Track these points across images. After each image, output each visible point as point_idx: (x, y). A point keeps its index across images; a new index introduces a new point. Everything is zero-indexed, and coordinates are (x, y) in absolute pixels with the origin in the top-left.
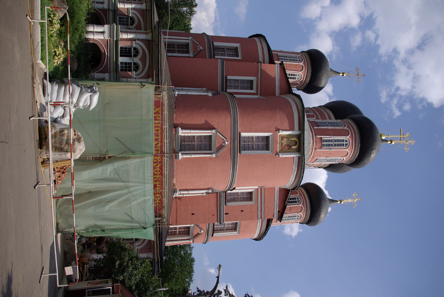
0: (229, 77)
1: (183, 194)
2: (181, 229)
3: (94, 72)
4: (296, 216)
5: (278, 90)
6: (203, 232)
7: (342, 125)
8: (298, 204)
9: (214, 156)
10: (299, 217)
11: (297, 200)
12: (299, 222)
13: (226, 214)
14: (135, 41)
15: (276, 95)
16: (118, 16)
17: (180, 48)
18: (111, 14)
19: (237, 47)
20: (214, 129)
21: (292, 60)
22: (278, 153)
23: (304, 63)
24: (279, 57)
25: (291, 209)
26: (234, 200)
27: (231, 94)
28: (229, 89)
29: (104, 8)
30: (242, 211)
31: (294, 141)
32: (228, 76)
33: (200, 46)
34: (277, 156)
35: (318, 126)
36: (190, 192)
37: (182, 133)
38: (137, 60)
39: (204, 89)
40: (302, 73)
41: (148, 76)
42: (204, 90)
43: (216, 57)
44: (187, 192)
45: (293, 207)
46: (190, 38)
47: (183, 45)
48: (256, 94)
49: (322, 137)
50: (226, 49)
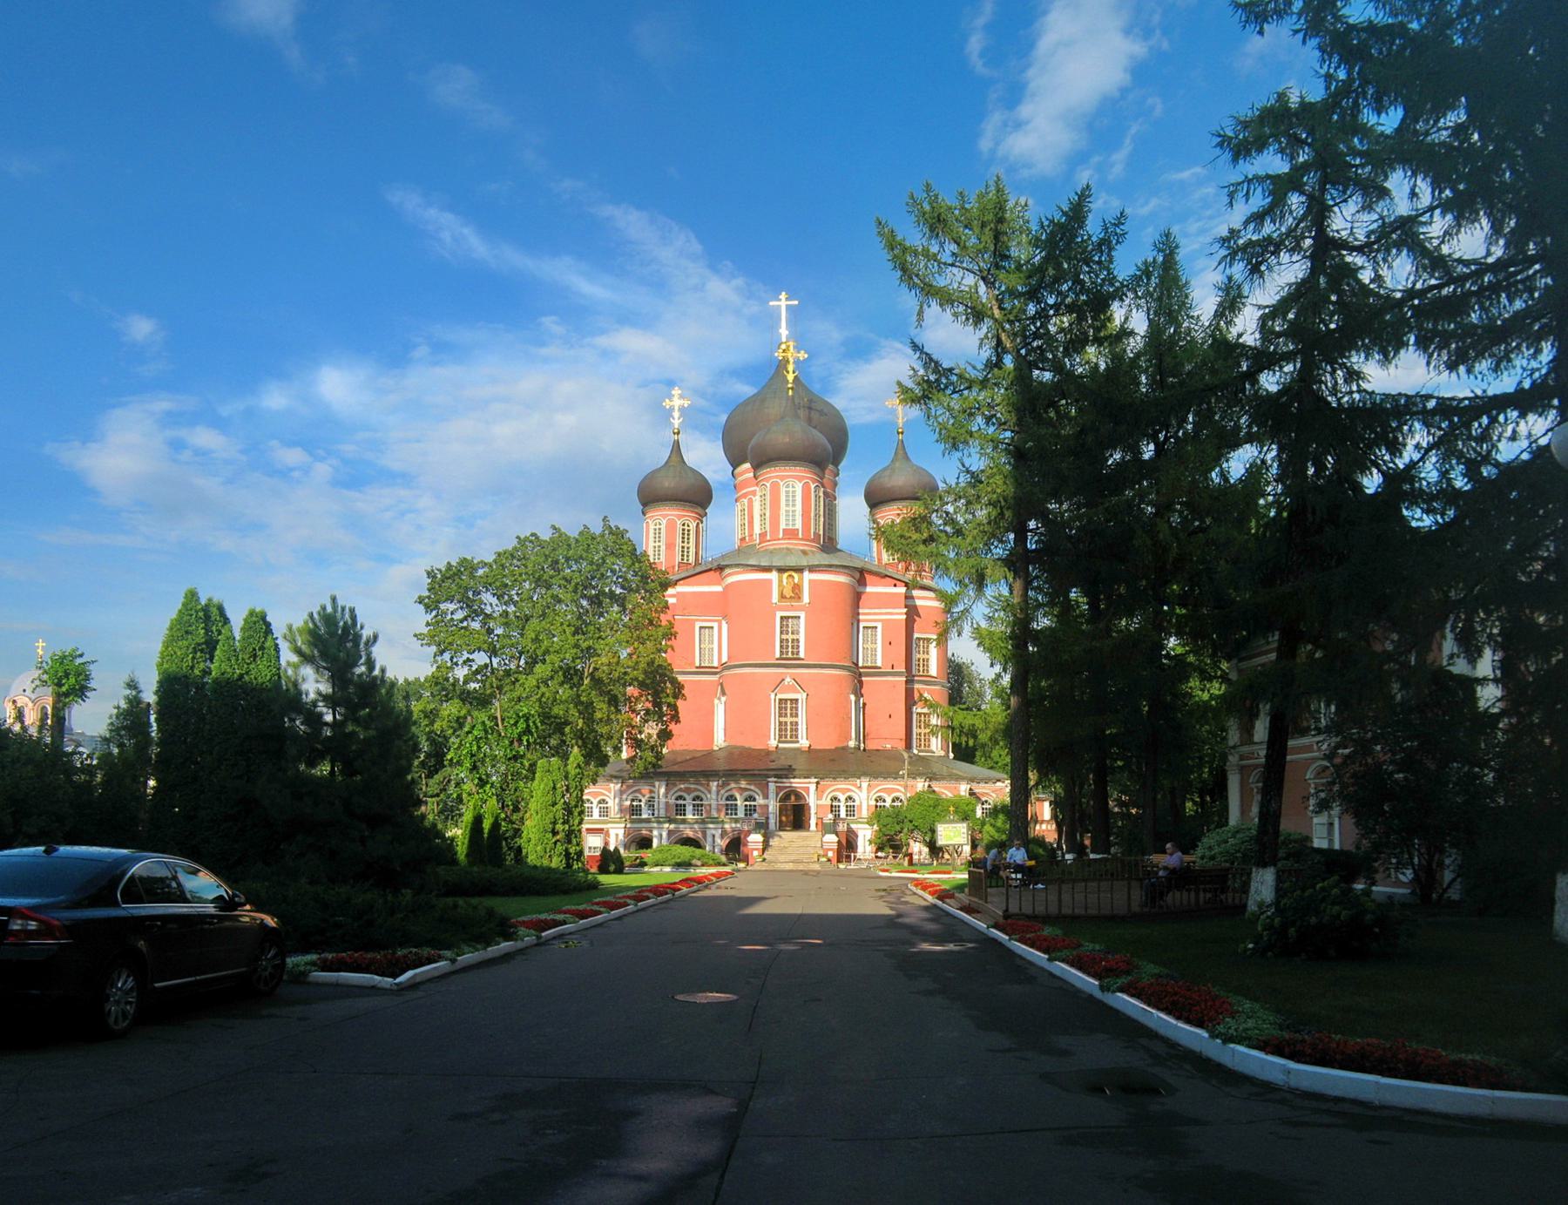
23: (664, 516)
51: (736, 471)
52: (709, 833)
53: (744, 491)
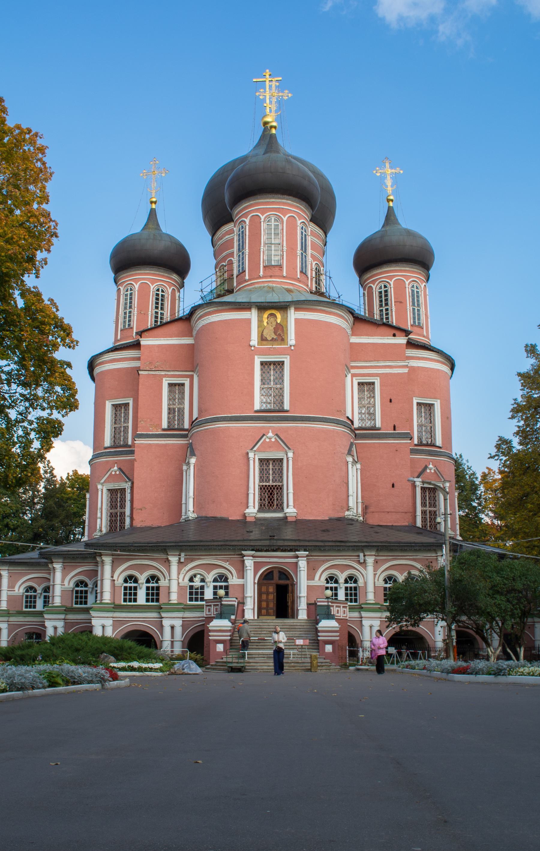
0: (165, 425)
1: (357, 502)
2: (425, 503)
3: (162, 641)
4: (413, 291)
5: (184, 339)
6: (432, 464)
7: (242, 227)
8: (391, 288)
9: (290, 455)
10: (415, 285)
11: (383, 290)
12: (424, 284)
13: (394, 429)
14: (114, 580)
15: (193, 342)
16: (75, 606)
17: (117, 504)
18: (70, 616)
19: (113, 405)
20: (248, 454)
21: (131, 303)
22: (289, 346)
24: (127, 327)
25: (399, 300)
26: (372, 415)
27: (192, 423)
28: (183, 424)
29: (63, 627)
30: (391, 401)
31: (269, 319)
32: (163, 427)
33: (112, 469)
34: (292, 348)
35: (245, 271)
36: (351, 492)
37: (254, 507)
38: (142, 578)
39: (185, 468)
40: (152, 285)
41: (165, 562)
42: (186, 469)
43: (130, 443)
44: (351, 498)
45: (394, 298)
46: (99, 487)
47: (111, 500)
48: (191, 377)
49: (263, 265)
50: (116, 426)
51: (216, 237)
52: (166, 623)
53: (224, 254)
